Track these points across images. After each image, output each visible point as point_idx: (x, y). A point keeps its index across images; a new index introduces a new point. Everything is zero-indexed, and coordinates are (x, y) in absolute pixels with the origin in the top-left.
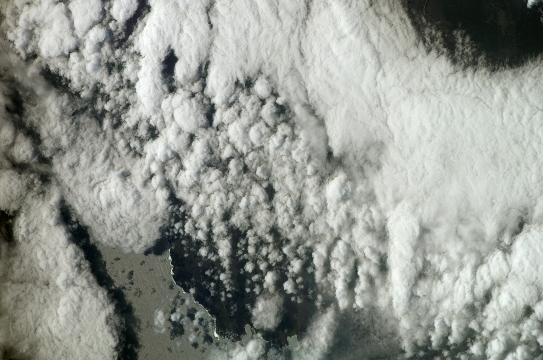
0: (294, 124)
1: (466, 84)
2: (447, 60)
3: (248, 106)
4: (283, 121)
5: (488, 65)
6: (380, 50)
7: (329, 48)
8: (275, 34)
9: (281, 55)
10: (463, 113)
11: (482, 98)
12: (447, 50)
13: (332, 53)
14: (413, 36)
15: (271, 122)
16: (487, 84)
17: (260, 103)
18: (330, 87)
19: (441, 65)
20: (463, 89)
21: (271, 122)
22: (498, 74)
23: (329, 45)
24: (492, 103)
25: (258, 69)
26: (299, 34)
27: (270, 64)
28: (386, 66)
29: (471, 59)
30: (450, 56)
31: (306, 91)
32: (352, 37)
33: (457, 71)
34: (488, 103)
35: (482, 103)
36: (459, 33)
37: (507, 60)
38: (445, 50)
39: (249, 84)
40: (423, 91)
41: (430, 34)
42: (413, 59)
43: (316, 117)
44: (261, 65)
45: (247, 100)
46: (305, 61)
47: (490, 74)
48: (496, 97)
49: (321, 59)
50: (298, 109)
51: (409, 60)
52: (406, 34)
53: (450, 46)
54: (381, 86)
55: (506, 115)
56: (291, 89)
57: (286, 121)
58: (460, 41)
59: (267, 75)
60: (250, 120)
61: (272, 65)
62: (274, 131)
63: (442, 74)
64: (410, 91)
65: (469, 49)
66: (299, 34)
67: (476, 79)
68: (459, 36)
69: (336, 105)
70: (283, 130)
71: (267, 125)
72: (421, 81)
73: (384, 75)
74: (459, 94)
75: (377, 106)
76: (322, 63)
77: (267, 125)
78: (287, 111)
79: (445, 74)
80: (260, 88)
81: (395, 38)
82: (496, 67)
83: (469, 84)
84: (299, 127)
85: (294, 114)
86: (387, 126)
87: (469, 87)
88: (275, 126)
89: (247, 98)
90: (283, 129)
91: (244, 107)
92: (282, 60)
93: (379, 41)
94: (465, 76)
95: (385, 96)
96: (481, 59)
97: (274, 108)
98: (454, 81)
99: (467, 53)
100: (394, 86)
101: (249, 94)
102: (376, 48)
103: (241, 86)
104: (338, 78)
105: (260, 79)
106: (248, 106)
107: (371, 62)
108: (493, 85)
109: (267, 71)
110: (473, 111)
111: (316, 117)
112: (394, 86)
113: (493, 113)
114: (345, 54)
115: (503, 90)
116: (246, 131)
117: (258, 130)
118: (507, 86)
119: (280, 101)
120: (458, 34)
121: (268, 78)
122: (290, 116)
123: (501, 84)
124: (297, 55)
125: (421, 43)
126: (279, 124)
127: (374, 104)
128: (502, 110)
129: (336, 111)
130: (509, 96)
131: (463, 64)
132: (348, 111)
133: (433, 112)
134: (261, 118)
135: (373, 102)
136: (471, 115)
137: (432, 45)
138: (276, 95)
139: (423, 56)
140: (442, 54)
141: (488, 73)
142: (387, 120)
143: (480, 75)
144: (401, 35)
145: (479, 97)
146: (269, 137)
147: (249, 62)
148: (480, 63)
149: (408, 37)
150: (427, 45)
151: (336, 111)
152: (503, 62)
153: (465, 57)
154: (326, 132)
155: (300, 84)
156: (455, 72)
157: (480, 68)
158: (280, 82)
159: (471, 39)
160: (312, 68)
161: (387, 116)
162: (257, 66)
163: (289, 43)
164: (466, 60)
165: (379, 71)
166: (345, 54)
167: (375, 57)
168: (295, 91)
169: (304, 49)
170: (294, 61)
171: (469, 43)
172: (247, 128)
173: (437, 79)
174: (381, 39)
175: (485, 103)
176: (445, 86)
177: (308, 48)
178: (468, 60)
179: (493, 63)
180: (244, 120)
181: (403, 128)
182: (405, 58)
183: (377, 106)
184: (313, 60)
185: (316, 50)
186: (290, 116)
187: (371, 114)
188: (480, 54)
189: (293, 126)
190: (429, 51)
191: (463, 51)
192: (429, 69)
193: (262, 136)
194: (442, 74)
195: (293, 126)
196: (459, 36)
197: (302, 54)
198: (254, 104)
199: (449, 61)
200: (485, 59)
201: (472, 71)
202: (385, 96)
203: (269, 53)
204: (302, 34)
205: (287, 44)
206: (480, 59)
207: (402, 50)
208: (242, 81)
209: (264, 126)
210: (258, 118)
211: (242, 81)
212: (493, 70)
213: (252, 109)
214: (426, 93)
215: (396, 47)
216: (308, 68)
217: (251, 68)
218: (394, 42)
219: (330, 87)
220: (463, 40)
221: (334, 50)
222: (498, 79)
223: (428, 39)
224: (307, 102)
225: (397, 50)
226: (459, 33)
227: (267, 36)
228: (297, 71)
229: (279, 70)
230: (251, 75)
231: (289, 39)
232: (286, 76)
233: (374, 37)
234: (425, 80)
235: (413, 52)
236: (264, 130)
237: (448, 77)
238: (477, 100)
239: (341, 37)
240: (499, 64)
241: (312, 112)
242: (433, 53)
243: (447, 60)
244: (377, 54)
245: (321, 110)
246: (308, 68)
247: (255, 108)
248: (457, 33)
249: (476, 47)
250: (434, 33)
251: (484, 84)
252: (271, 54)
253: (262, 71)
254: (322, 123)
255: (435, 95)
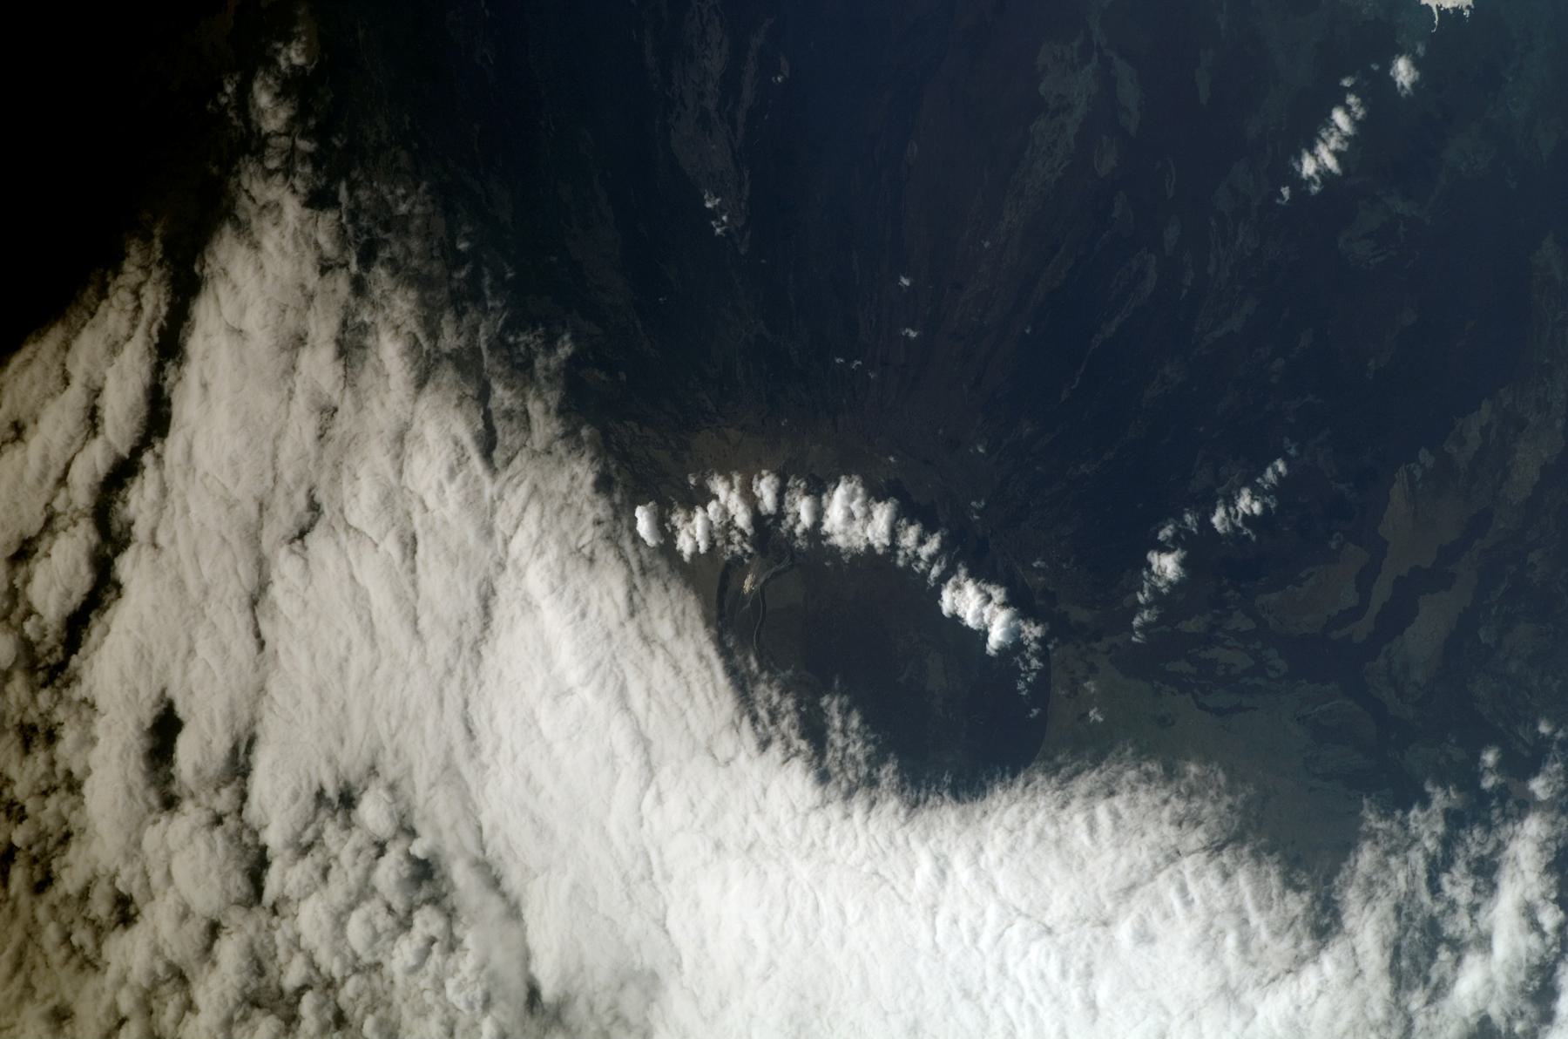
0: (454, 909)
1: (850, 835)
2: (807, 771)
3: (346, 856)
4: (427, 901)
5: (903, 790)
6: (651, 735)
7: (532, 721)
8: (408, 676)
9: (423, 730)
10: (842, 912)
11: (888, 875)
12: (810, 744)
13: (540, 732)
14: (727, 702)
15: (399, 904)
16: (899, 839)
17: (373, 851)
18: (534, 821)
19: (792, 783)
20: (843, 849)
21: (399, 904)
22: (926, 813)
23: (533, 712)
24: (911, 891)
25: (369, 763)
26: (464, 679)
27: (396, 753)
28: (665, 775)
29: (864, 770)
30: (815, 763)
31: (480, 828)
32: (587, 694)
33: (829, 802)
34: (901, 889)
35: (885, 888)
36: (835, 702)
37: (947, 779)
38: (803, 745)
39: (348, 800)
40: (751, 846)
41: (768, 699)
42: (727, 763)
43: (504, 895)
44: (375, 754)
45: (343, 842)
46: (478, 749)
47: (908, 814)
48: (918, 873)
49: (512, 748)
50: (461, 875)
51: (718, 765)
52: (711, 694)
53: (814, 732)
54: (651, 829)
55: (942, 921)
56: (445, 820)
57: (435, 901)
58: (837, 723)
59: (390, 779)
60: (349, 894)
61: (401, 755)
62: (405, 925)
63: (793, 807)
64: (718, 846)
65: (859, 745)
66: (464, 679)
67: (872, 825)
68: (834, 710)
69: (547, 868)
70: (426, 924)
71: (390, 909)
72: (746, 820)
73: (659, 798)
74: (833, 861)
75: (643, 879)
76: (515, 757)
77: (390, 909)
78: (436, 876)
79: (801, 809)
80: (373, 812)
81: (686, 705)
82: (922, 796)
83: (856, 837)
84: (464, 920)
85: (452, 887)
86: (667, 932)
87: (856, 846)
88: (410, 913)
89: (344, 834)
90: (427, 922)
91: (336, 858)
92: (423, 743)
93: (648, 709)
94: (847, 816)
95: (661, 854)
96: (887, 773)
97: (406, 865)
98: (821, 826)
99: (853, 757)
100: (682, 829)
101: (348, 825)
102: (643, 727)
103: (329, 803)
104: (551, 799)
105: (372, 788)
106: (346, 856)
107: (630, 761)
108: (914, 844)
109: (390, 771)
110: (866, 906)
111: (504, 895)
112: (682, 829)
113: (912, 917)
114: (570, 738)
115: (937, 859)
116: (340, 920)
117: (368, 920)
118: (944, 848)
119: (419, 849)
120: (832, 705)
121: (392, 787)
122: (444, 889)
123: (932, 842)
124: (458, 733)
125: (746, 720)
126: (419, 907)
127: (635, 874)
128: (933, 910)
129: (546, 884)
130: (949, 873)
131: (844, 785)
132: (575, 887)
133: (771, 905)
134: (374, 890)
135: (633, 866)
136: (861, 919)
137: (771, 729)
138: (412, 833)
139: (750, 757)
140: (798, 753)
141: (902, 812)
142: (665, 917)
143: (884, 813)
144: (700, 698)
145: (881, 872)
146: (394, 939)
147: (347, 743)
148: (884, 782)
149: (715, 703)
150: (760, 729)
151: (546, 884)
152: (938, 782)
153: (849, 765)
154: (524, 938)
155: (465, 808)
156: (825, 802)
157: (884, 796)
158: (419, 800)
159: (863, 722)
160: (493, 768)
161: (666, 907)
162: (366, 756)
163: (441, 701)
164: (850, 775)
165: (648, 786)
166: (570, 738)
167: (639, 749)
168: (453, 828)
169: (475, 718)
170: (452, 749)
171: (858, 731)
172: (341, 914)
173: (782, 822)
174: (654, 707)
175: (893, 888)
176: (800, 838)
177: (484, 717)
178: (856, 775)
179: (916, 784)
180: (337, 891)
181: (703, 942)
182: (710, 759)
183: (643, 879)
184: (497, 748)
185: (502, 719)
186: (444, 889)
187: (629, 897)
188: (885, 760)
189: (451, 915)
190: (764, 744)
191: (845, 749)
192: (765, 791)
193: (376, 936)
194: (793, 807)
195: (451, 915)
196: (834, 710)
197: (470, 731)
198: (359, 851)
199: (811, 775)
200: (895, 772)
201: (866, 802)
202: (661, 854)
203: (394, 723)
204: (471, 679)
205: (435, 700)
206: (883, 773)
207: (701, 737)
208: (331, 792)
209: (383, 911)
210: (365, 891)
211: (331, 792)
212: (914, 805)
213: (355, 864)
214: (756, 854)
215: (688, 727)
216: (484, 767)
217: (352, 761)
218: (683, 714)
219: (534, 821)
220: (845, 723)
221: (545, 725)
222: (926, 827)
223: (763, 713)
224: (480, 855)
225: (691, 735)
226: (835, 702)
227: (390, 680)
228: (459, 775)
229: (416, 769)
230: (352, 778)
231: (441, 690)
232: (432, 785)
233: (638, 701)
234: (753, 817)
235: (726, 745)
236: (383, 921)
237: (807, 815)
238: (875, 879)
239: (561, 694)
240: (928, 788)
241: (495, 883)
242: (776, 750)
243: (807, 771)
244: (644, 743)
245: (513, 880)
246: (484, 767)
247: (362, 863)
248: (829, 704)
249: (875, 742)
250: (775, 699)
251: (891, 841)
252: (399, 727)
253: (378, 769)
254: (514, 913)
255: (777, 860)
